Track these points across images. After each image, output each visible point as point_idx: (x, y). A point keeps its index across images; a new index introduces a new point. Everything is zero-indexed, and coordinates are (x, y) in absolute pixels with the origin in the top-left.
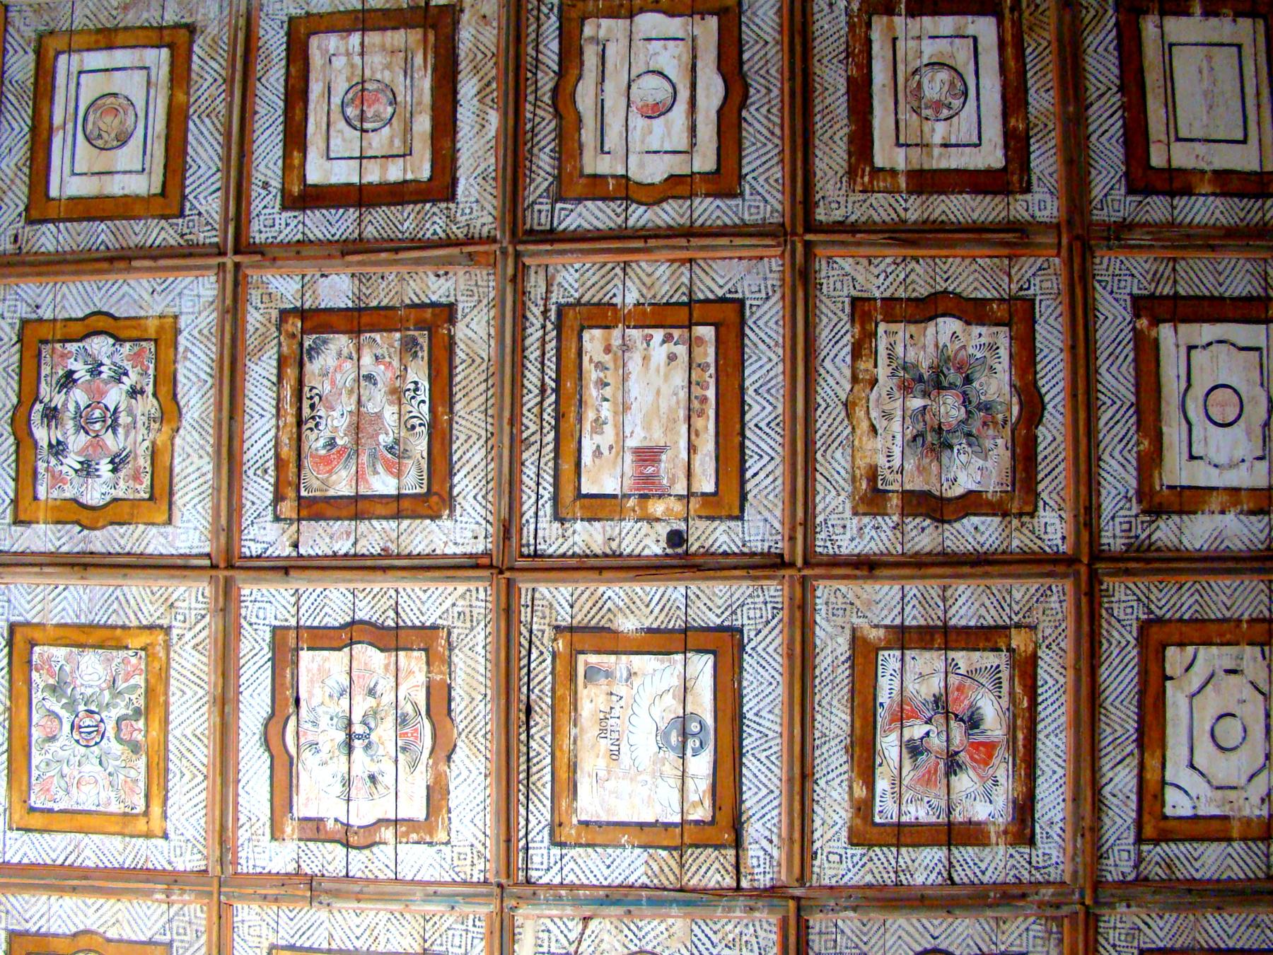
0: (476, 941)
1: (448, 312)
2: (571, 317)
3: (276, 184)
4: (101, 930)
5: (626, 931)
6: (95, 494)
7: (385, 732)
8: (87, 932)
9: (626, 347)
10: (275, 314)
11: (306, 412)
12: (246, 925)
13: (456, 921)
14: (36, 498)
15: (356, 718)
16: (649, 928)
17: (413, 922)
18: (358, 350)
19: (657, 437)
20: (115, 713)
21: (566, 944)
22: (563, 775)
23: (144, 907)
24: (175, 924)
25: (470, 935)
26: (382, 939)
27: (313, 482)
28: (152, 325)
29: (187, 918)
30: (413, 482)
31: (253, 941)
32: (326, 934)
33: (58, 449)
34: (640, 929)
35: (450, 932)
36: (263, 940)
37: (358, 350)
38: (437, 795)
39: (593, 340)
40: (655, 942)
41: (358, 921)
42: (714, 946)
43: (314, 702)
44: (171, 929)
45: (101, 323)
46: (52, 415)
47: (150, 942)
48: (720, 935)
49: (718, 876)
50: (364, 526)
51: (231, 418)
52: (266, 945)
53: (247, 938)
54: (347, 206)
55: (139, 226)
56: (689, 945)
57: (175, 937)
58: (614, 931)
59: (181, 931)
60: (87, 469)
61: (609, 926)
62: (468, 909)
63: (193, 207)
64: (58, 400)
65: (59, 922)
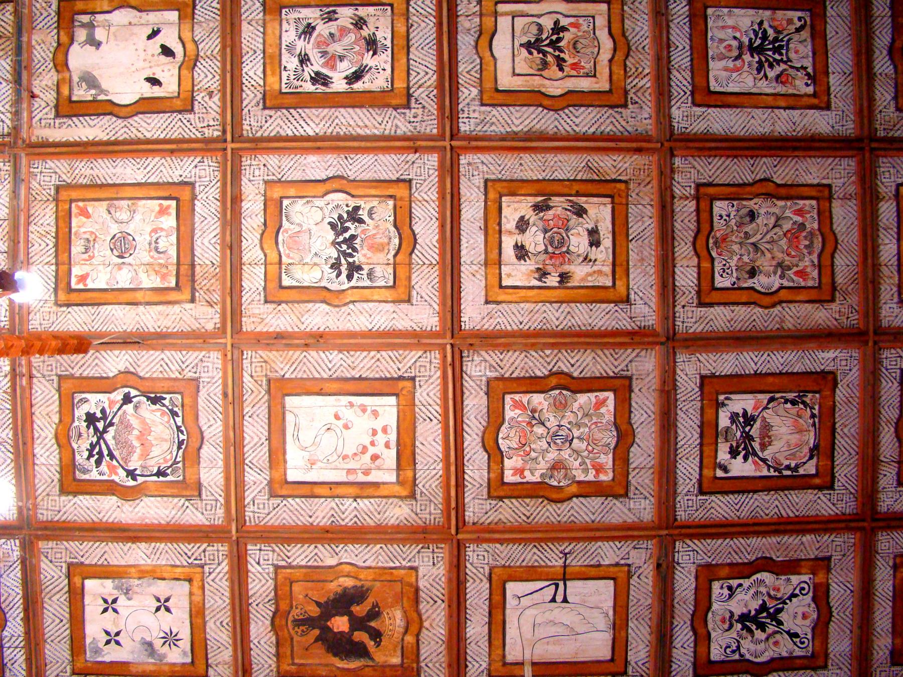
0: (47, 166)
4: (54, 426)
5: (40, 70)
8: (56, 437)
12: (43, 322)
13: (35, 180)
16: (38, 56)
17: (36, 208)
21: (49, 108)
23: (37, 394)
24: (46, 373)
25: (44, 170)
26: (48, 229)
29: (41, 364)
31: (53, 317)
32: (46, 267)
34: (39, 61)
35: (42, 183)
36: (52, 310)
40: (48, 52)
41: (37, 245)
42: (49, 15)
44: (49, 376)
47: (59, 390)
48: (43, 11)
49: (7, 14)
52: (55, 308)
53: (51, 321)
56: (49, 30)
57: (54, 373)
58: (41, 78)
59: (50, 368)
61: (38, 82)
62: (24, 170)
65: (51, 457)
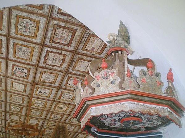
1: (76, 30)
2: (90, 35)
3: (57, 11)
6: (26, 34)
7: (57, 60)
9: (96, 39)
10: (53, 24)
11: (55, 34)
14: (18, 32)
15: (55, 58)
18: (64, 30)
19: (95, 47)
20: (27, 52)
22: (75, 66)
27: (54, 40)
28: (36, 21)
30: (66, 43)
33: (21, 29)
37: (64, 30)
38: (61, 65)
39: (92, 38)
43: (50, 56)
45: (29, 18)
46: (20, 25)
50: (60, 45)
51: (46, 33)
54: (66, 16)
55: (36, 9)
60: (25, 32)
63: (44, 9)
64: (22, 24)
